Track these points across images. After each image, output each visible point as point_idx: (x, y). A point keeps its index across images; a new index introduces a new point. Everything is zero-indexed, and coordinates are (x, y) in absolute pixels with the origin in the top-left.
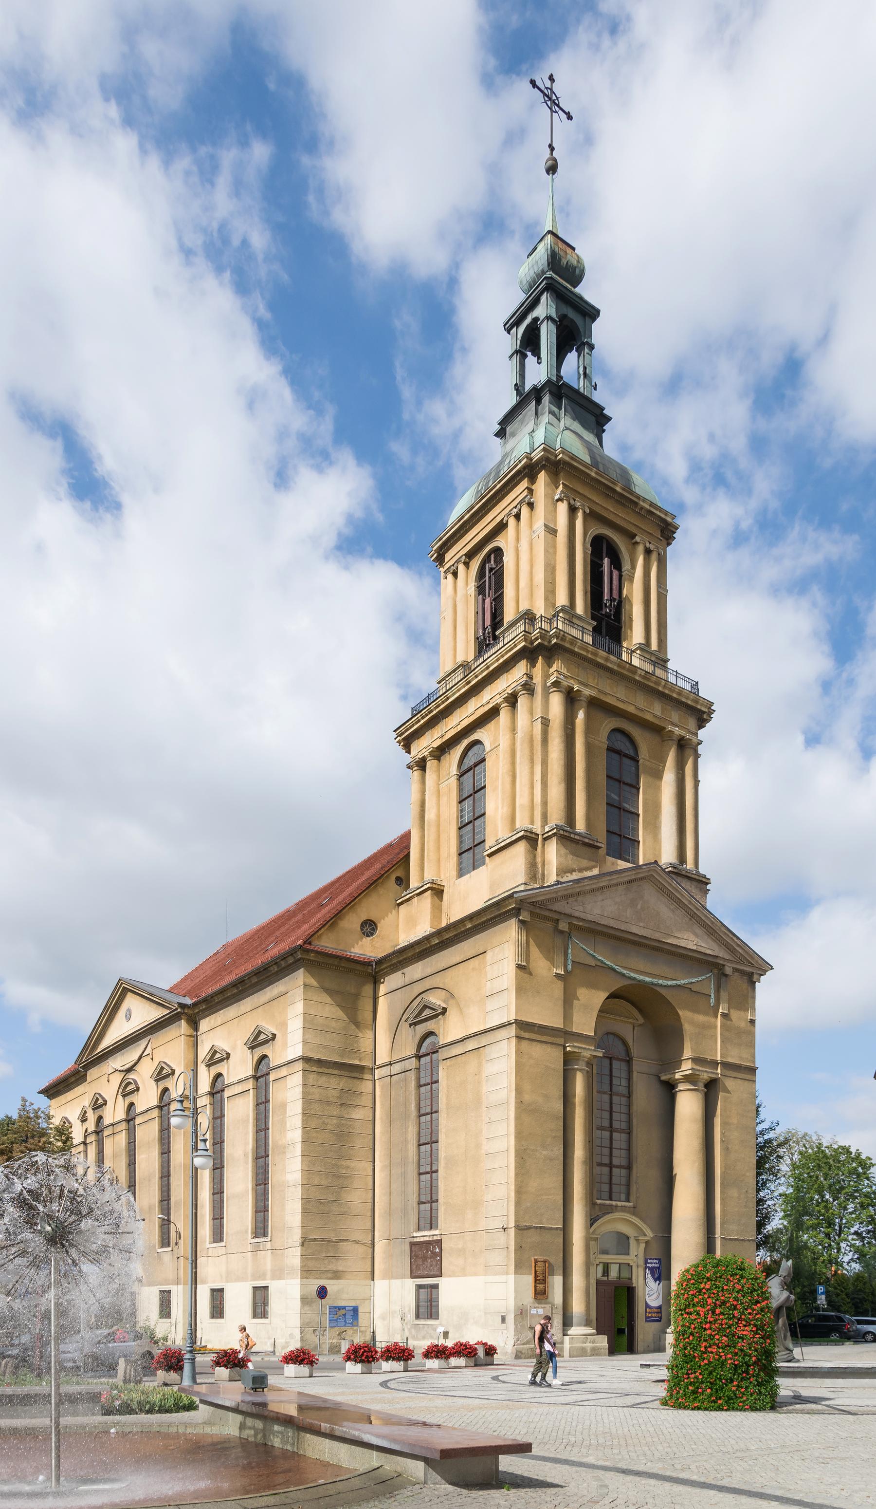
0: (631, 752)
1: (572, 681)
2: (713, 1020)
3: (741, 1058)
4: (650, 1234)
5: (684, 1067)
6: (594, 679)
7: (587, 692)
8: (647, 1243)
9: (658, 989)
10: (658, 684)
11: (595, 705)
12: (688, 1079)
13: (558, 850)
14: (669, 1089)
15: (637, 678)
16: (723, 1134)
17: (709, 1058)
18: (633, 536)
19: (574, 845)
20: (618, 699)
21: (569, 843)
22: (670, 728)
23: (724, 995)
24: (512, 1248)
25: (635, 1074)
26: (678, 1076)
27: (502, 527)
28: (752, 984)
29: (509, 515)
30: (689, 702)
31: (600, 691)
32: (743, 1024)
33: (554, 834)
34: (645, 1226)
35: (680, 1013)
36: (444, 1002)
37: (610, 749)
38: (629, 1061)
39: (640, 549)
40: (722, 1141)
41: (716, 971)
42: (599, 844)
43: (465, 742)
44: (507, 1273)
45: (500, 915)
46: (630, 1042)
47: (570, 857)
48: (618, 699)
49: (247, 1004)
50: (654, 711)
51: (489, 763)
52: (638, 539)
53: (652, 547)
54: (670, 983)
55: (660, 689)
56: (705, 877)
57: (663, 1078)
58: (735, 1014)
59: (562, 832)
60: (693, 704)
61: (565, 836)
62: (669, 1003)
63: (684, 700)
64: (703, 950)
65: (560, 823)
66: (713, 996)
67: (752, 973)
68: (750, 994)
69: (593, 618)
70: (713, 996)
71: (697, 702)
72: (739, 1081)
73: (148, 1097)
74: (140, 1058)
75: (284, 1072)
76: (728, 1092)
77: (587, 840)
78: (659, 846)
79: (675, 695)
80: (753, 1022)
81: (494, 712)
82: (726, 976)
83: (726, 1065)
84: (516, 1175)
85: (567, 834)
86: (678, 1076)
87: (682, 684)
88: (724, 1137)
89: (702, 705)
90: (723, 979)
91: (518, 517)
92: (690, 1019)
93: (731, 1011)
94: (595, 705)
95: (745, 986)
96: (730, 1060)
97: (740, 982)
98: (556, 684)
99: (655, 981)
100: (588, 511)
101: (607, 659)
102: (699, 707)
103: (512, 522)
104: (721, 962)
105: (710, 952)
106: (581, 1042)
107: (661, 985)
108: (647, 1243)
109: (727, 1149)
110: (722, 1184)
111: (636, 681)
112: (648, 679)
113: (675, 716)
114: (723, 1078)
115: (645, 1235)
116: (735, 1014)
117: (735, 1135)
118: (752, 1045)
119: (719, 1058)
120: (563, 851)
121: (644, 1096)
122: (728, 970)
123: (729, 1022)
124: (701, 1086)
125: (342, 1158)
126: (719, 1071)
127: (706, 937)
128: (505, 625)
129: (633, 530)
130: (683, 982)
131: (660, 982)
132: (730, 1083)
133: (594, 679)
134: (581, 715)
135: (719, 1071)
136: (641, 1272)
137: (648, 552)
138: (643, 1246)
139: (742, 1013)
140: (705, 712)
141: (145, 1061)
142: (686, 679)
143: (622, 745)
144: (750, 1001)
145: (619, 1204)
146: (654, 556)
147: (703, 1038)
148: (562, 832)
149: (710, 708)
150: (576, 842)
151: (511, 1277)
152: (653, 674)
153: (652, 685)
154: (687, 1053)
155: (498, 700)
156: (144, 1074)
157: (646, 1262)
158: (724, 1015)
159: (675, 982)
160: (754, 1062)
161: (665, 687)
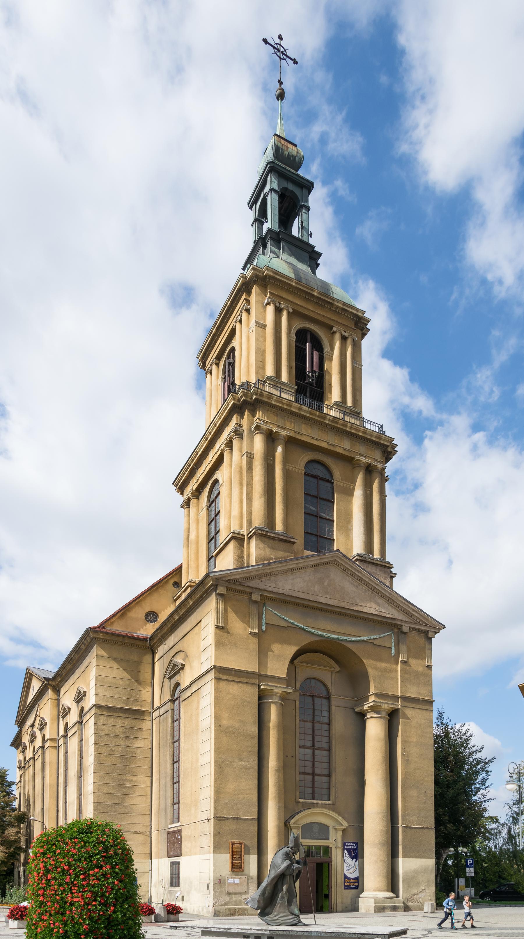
1: (272, 426)
2: (394, 666)
3: (419, 694)
5: (370, 701)
6: (291, 424)
7: (283, 433)
10: (346, 426)
11: (291, 442)
12: (373, 709)
13: (257, 545)
15: (327, 422)
16: (403, 750)
17: (390, 693)
19: (271, 542)
20: (312, 438)
21: (266, 540)
22: (358, 457)
23: (403, 648)
26: (366, 707)
28: (429, 639)
30: (373, 439)
31: (296, 432)
32: (421, 669)
33: (254, 533)
34: (340, 817)
35: (365, 661)
40: (402, 755)
41: (396, 630)
42: (293, 540)
45: (206, 591)
47: (268, 550)
48: (312, 438)
50: (343, 446)
55: (348, 429)
58: (413, 662)
59: (260, 532)
60: (377, 440)
61: (265, 534)
62: (355, 654)
63: (369, 437)
64: (384, 615)
65: (260, 526)
66: (393, 648)
67: (428, 631)
68: (427, 646)
70: (393, 648)
71: (380, 438)
72: (418, 711)
76: (408, 718)
77: (282, 537)
79: (360, 434)
80: (430, 667)
82: (405, 633)
83: (405, 699)
85: (264, 533)
86: (366, 707)
88: (405, 751)
89: (384, 440)
90: (403, 636)
92: (372, 667)
93: (410, 660)
94: (291, 442)
96: (409, 695)
97: (417, 639)
98: (258, 428)
102: (382, 442)
105: (390, 616)
106: (278, 683)
108: (344, 830)
109: (408, 760)
110: (403, 786)
111: (326, 424)
112: (337, 423)
113: (362, 449)
114: (403, 708)
116: (413, 662)
117: (414, 751)
118: (429, 683)
119: (399, 694)
120: (262, 545)
123: (408, 668)
124: (384, 714)
126: (400, 703)
127: (387, 605)
132: (409, 712)
133: (291, 424)
134: (279, 449)
135: (400, 703)
136: (339, 852)
139: (420, 661)
140: (388, 446)
144: (427, 652)
147: (386, 679)
148: (260, 532)
149: (391, 442)
150: (274, 539)
153: (341, 427)
154: (372, 690)
157: (344, 844)
158: (403, 662)
160: (431, 696)
161: (351, 428)
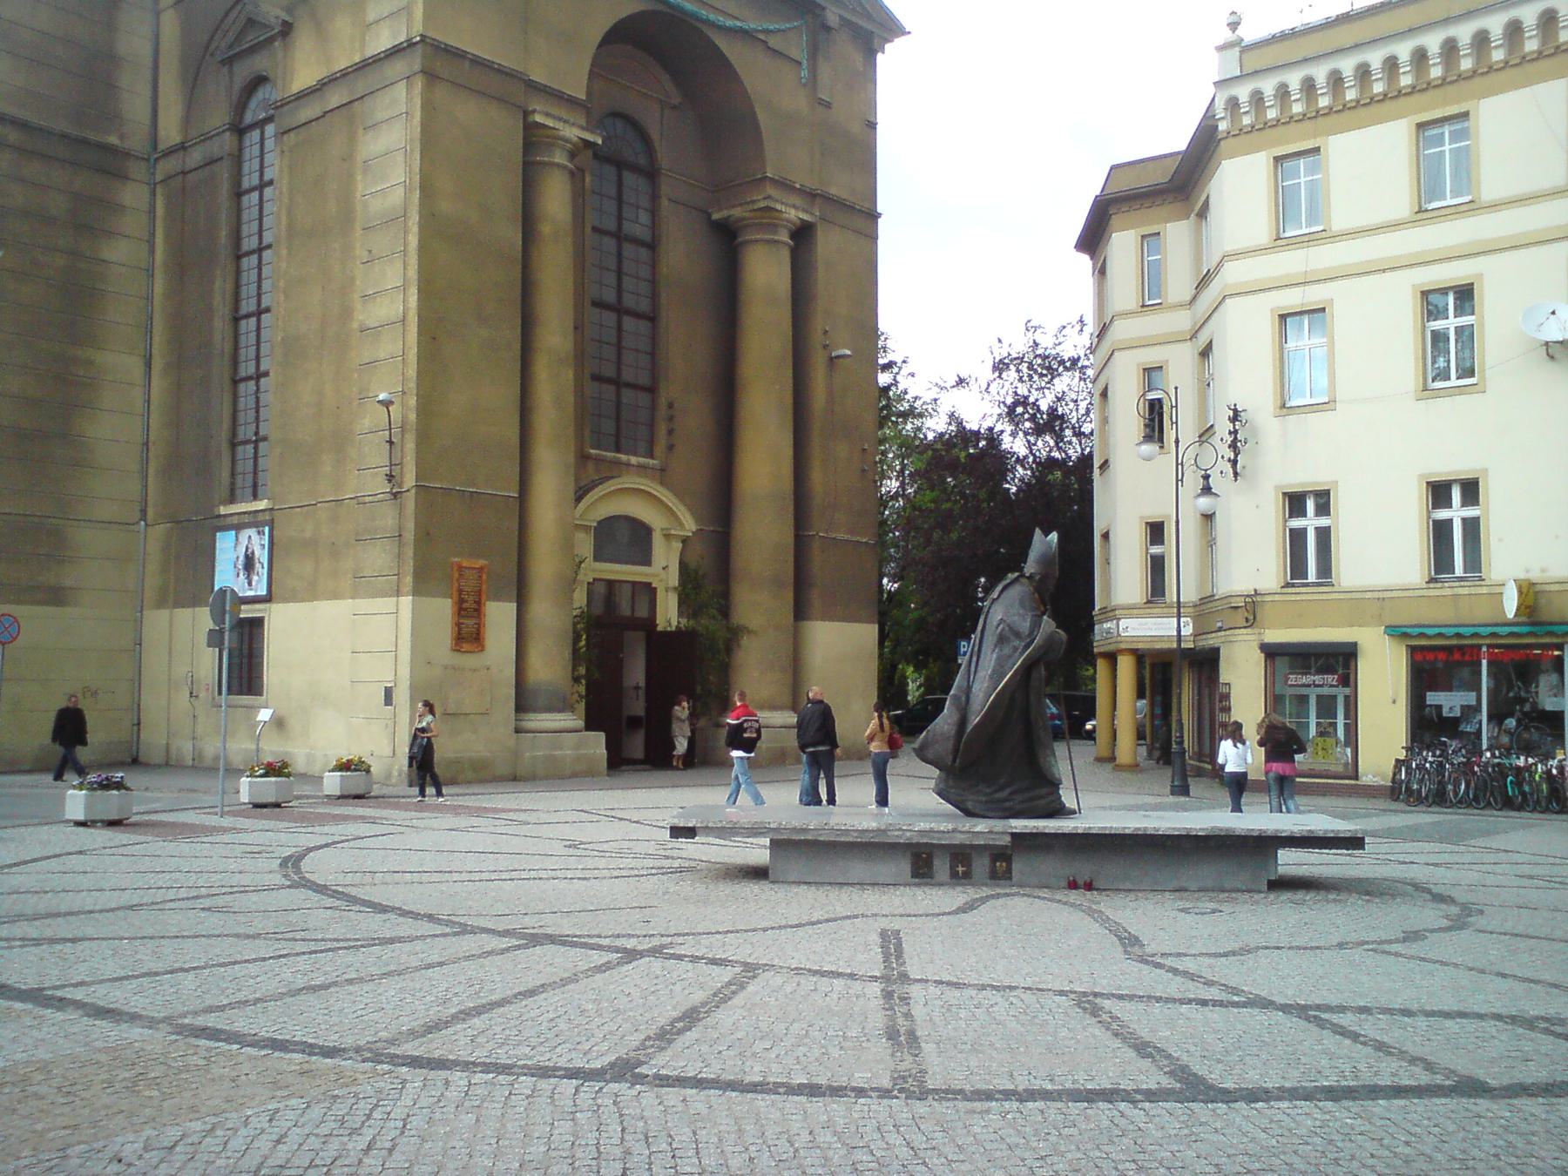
4: (690, 525)
8: (685, 541)
14: (728, 241)
24: (409, 535)
25: (665, 202)
38: (651, 174)
44: (398, 593)
54: (729, 23)
57: (715, 216)
82: (827, 28)
84: (420, 373)
99: (704, 13)
107: (713, 25)
115: (681, 525)
130: (753, 26)
131: (712, 17)
138: (678, 546)
145: (634, 460)
151: (406, 601)
159: (739, 24)
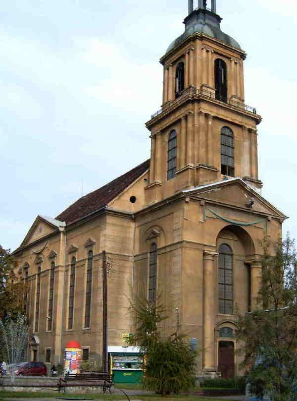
0: (230, 134)
9: (241, 226)
18: (231, 58)
27: (183, 56)
29: (185, 53)
36: (159, 231)
37: (222, 134)
39: (233, 63)
43: (170, 130)
46: (232, 247)
49: (86, 228)
50: (238, 119)
51: (177, 137)
52: (232, 59)
53: (237, 62)
56: (260, 181)
69: (215, 88)
73: (46, 266)
74: (44, 248)
75: (97, 258)
78: (242, 170)
81: (179, 121)
87: (249, 110)
91: (189, 53)
95: (277, 224)
100: (213, 51)
101: (220, 103)
103: (187, 55)
104: (267, 215)
121: (239, 271)
122: (270, 218)
125: (119, 294)
128: (185, 89)
129: (230, 57)
137: (236, 63)
141: (46, 250)
142: (251, 108)
143: (227, 132)
146: (238, 65)
152: (238, 107)
155: (181, 117)
156: (46, 254)
